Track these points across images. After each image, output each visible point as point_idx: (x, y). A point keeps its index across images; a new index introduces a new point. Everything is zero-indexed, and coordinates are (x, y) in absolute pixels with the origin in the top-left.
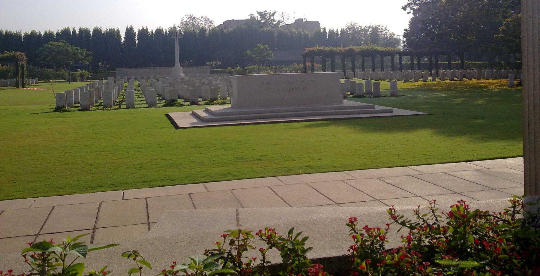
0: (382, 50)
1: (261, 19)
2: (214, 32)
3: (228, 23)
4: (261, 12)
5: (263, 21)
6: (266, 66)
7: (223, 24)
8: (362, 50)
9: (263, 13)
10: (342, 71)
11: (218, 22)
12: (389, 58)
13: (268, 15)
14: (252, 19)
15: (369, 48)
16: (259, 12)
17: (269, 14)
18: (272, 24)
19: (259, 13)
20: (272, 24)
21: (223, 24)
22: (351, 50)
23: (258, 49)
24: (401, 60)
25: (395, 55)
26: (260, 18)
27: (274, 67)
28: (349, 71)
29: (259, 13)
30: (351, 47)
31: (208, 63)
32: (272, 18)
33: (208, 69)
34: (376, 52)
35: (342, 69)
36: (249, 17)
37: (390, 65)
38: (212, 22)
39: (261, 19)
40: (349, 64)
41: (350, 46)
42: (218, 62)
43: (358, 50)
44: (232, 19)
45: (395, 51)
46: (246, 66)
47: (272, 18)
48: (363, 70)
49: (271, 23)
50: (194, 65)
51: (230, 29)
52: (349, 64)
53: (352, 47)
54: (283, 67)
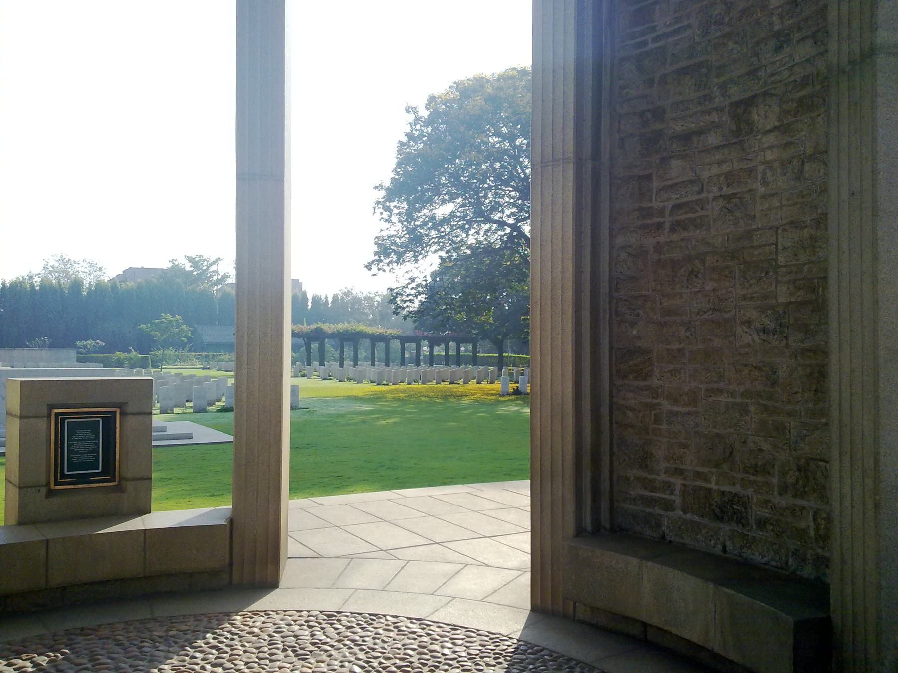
0: (370, 332)
1: (192, 269)
2: (100, 290)
3: (131, 273)
4: (194, 257)
5: (195, 273)
6: (188, 352)
7: (122, 273)
8: (347, 331)
9: (197, 259)
10: (338, 364)
11: (112, 271)
12: (414, 345)
13: (205, 263)
14: (176, 270)
15: (349, 329)
16: (187, 257)
17: (208, 261)
18: (211, 279)
19: (190, 259)
20: (211, 279)
21: (122, 273)
22: (319, 331)
23: (162, 322)
24: (431, 351)
25: (392, 341)
26: (191, 266)
27: (204, 354)
28: (348, 363)
29: (190, 259)
30: (319, 325)
31: (78, 343)
32: (213, 268)
33: (73, 354)
34: (362, 335)
35: (319, 359)
36: (170, 265)
37: (383, 356)
38: (103, 269)
39: (192, 269)
40: (348, 352)
41: (318, 324)
42: (98, 341)
43: (330, 331)
44: (140, 267)
45: (391, 334)
46: (151, 351)
47: (213, 268)
48: (387, 365)
49: (211, 277)
50: (52, 346)
51: (130, 284)
52: (348, 352)
53: (320, 324)
54: (220, 355)
